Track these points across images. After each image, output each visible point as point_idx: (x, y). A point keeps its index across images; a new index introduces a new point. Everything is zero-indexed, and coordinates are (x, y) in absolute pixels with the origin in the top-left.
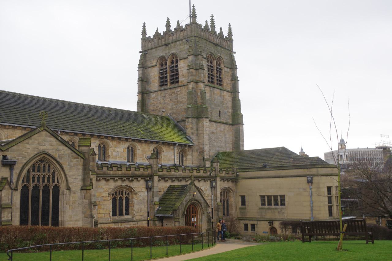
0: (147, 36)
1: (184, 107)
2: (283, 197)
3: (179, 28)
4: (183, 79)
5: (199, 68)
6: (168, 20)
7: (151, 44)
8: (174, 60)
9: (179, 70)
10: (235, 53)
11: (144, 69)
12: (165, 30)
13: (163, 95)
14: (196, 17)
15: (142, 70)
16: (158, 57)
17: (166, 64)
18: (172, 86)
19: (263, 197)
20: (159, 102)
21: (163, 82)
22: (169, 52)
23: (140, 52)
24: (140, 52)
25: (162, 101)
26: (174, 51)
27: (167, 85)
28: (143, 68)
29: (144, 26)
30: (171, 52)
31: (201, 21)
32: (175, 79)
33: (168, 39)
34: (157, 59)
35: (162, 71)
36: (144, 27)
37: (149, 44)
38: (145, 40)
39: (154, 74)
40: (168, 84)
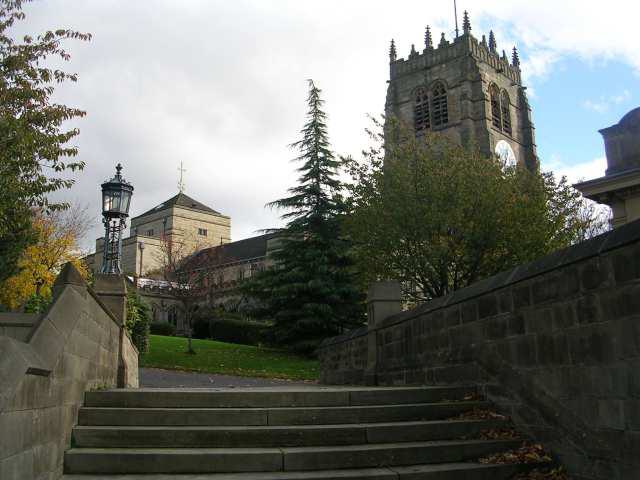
10: (525, 88)
12: (424, 47)
17: (426, 98)
18: (437, 127)
31: (477, 33)
36: (393, 46)
38: (396, 65)
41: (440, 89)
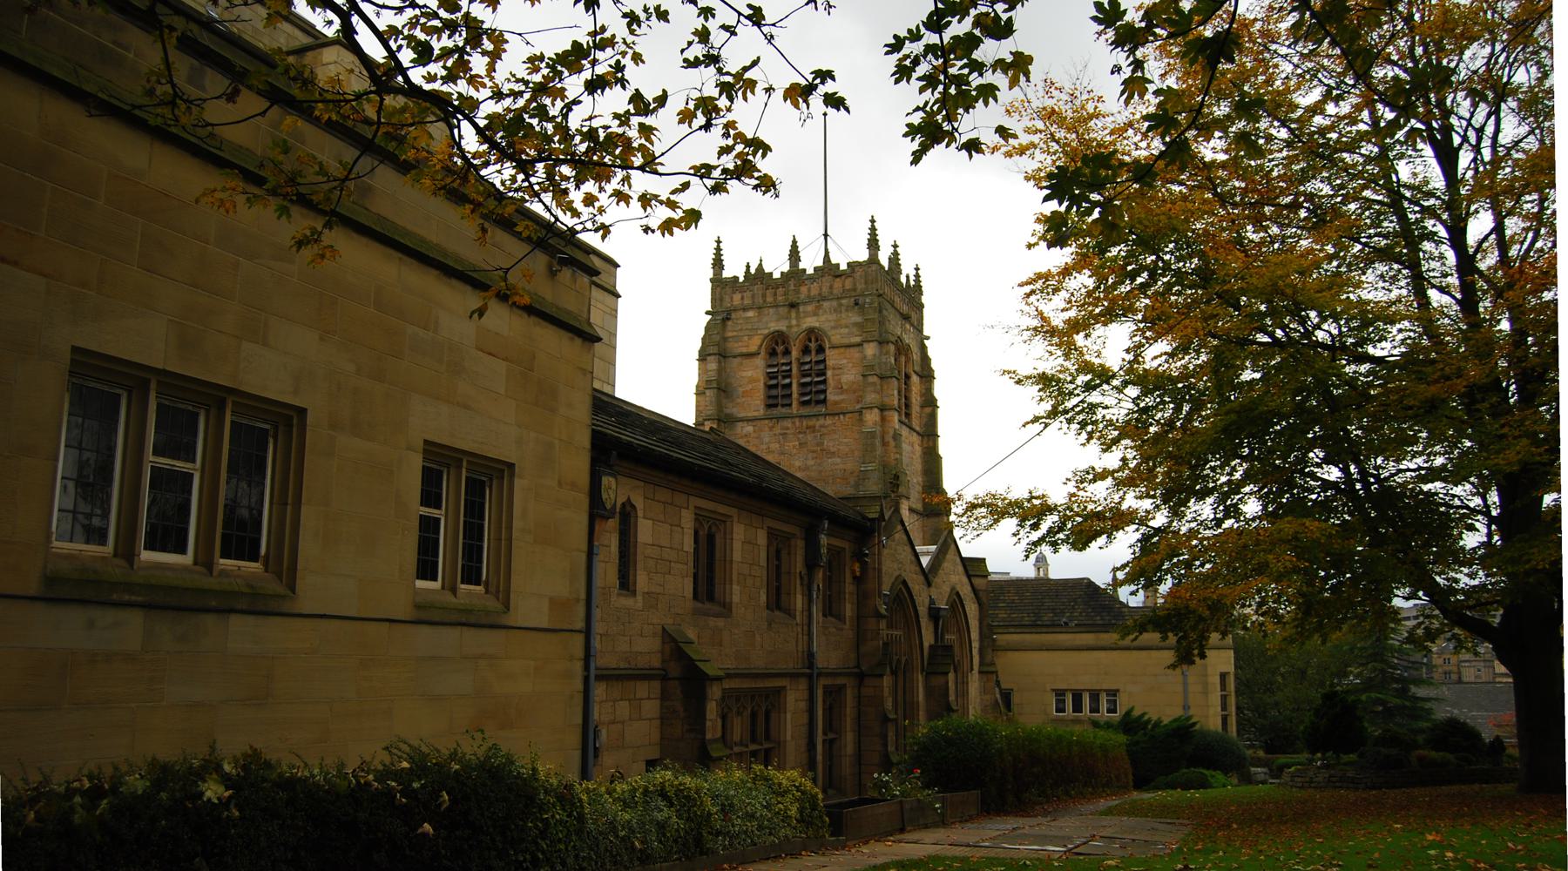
0: (727, 274)
1: (841, 466)
2: (1113, 693)
3: (828, 268)
4: (837, 398)
5: (888, 374)
6: (794, 242)
7: (742, 298)
8: (813, 345)
9: (829, 373)
11: (721, 358)
13: (778, 430)
14: (878, 248)
15: (719, 362)
16: (766, 331)
17: (787, 352)
18: (805, 411)
19: (1060, 694)
20: (764, 447)
21: (776, 396)
22: (798, 325)
23: (707, 313)
24: (707, 313)
25: (775, 446)
26: (817, 325)
27: (790, 405)
28: (720, 354)
29: (718, 246)
30: (804, 326)
32: (815, 394)
33: (797, 292)
34: (762, 337)
35: (776, 370)
37: (734, 296)
38: (721, 286)
39: (751, 376)
40: (795, 404)
41: (815, 342)
